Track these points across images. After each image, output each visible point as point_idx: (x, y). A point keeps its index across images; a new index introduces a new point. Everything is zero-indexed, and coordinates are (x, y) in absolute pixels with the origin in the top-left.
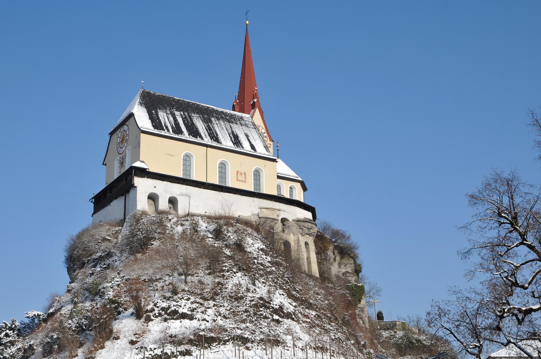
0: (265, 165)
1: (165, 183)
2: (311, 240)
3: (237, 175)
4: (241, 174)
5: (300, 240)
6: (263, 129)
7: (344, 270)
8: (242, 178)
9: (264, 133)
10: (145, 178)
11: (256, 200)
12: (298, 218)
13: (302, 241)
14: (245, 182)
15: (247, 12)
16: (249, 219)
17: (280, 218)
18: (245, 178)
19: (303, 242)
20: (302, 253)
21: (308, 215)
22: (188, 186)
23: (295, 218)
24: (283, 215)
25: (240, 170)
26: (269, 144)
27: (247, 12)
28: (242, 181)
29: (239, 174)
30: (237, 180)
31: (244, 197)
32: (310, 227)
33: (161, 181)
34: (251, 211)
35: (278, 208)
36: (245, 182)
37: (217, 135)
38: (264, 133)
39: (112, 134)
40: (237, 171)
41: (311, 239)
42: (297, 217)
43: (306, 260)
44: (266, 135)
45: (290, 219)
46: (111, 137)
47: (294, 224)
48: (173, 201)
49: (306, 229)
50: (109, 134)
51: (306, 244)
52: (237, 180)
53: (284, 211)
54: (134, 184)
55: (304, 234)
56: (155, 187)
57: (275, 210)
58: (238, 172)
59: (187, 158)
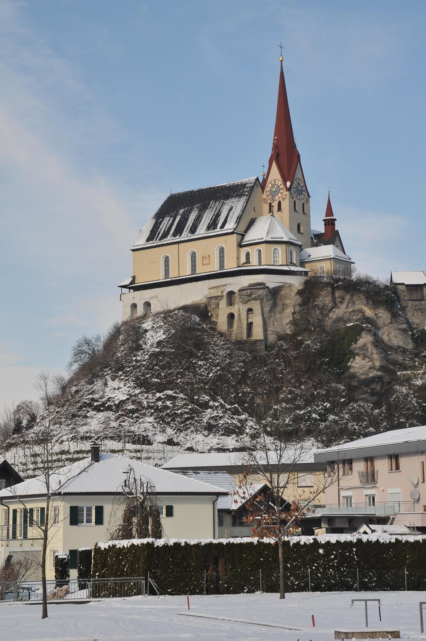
7: (350, 309)
9: (281, 185)
11: (207, 282)
16: (200, 302)
17: (225, 293)
23: (239, 288)
24: (228, 289)
28: (207, 264)
29: (204, 258)
30: (203, 265)
37: (200, 223)
38: (281, 185)
42: (242, 286)
48: (148, 305)
49: (245, 296)
52: (203, 265)
53: (229, 284)
55: (244, 302)
56: (134, 298)
58: (203, 256)
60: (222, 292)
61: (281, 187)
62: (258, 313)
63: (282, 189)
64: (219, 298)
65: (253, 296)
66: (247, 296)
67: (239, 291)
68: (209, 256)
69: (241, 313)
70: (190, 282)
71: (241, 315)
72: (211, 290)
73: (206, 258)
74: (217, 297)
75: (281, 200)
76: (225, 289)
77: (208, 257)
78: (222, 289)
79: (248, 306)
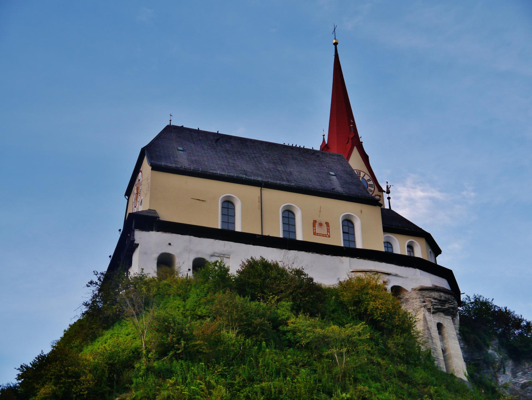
0: (361, 211)
1: (186, 238)
2: (449, 321)
3: (314, 226)
4: (321, 225)
5: (428, 319)
6: (366, 175)
9: (369, 180)
10: (152, 231)
11: (346, 260)
12: (421, 286)
13: (431, 321)
14: (327, 236)
15: (335, 29)
17: (389, 287)
18: (328, 231)
19: (433, 323)
20: (432, 339)
21: (443, 283)
22: (226, 242)
23: (417, 285)
24: (394, 282)
25: (319, 220)
26: (377, 195)
27: (335, 29)
28: (323, 235)
30: (315, 234)
31: (325, 256)
32: (443, 298)
33: (179, 235)
34: (337, 278)
36: (327, 236)
39: (128, 193)
40: (314, 221)
41: (450, 319)
43: (440, 352)
44: (371, 183)
45: (409, 289)
46: (128, 200)
47: (414, 295)
50: (125, 196)
51: (440, 326)
52: (315, 234)
54: (134, 241)
57: (380, 274)
58: (315, 222)
61: (369, 183)
62: (453, 336)
63: (371, 186)
65: (447, 306)
66: (439, 300)
68: (327, 224)
69: (429, 326)
70: (306, 251)
71: (430, 329)
77: (325, 225)
78: (386, 278)
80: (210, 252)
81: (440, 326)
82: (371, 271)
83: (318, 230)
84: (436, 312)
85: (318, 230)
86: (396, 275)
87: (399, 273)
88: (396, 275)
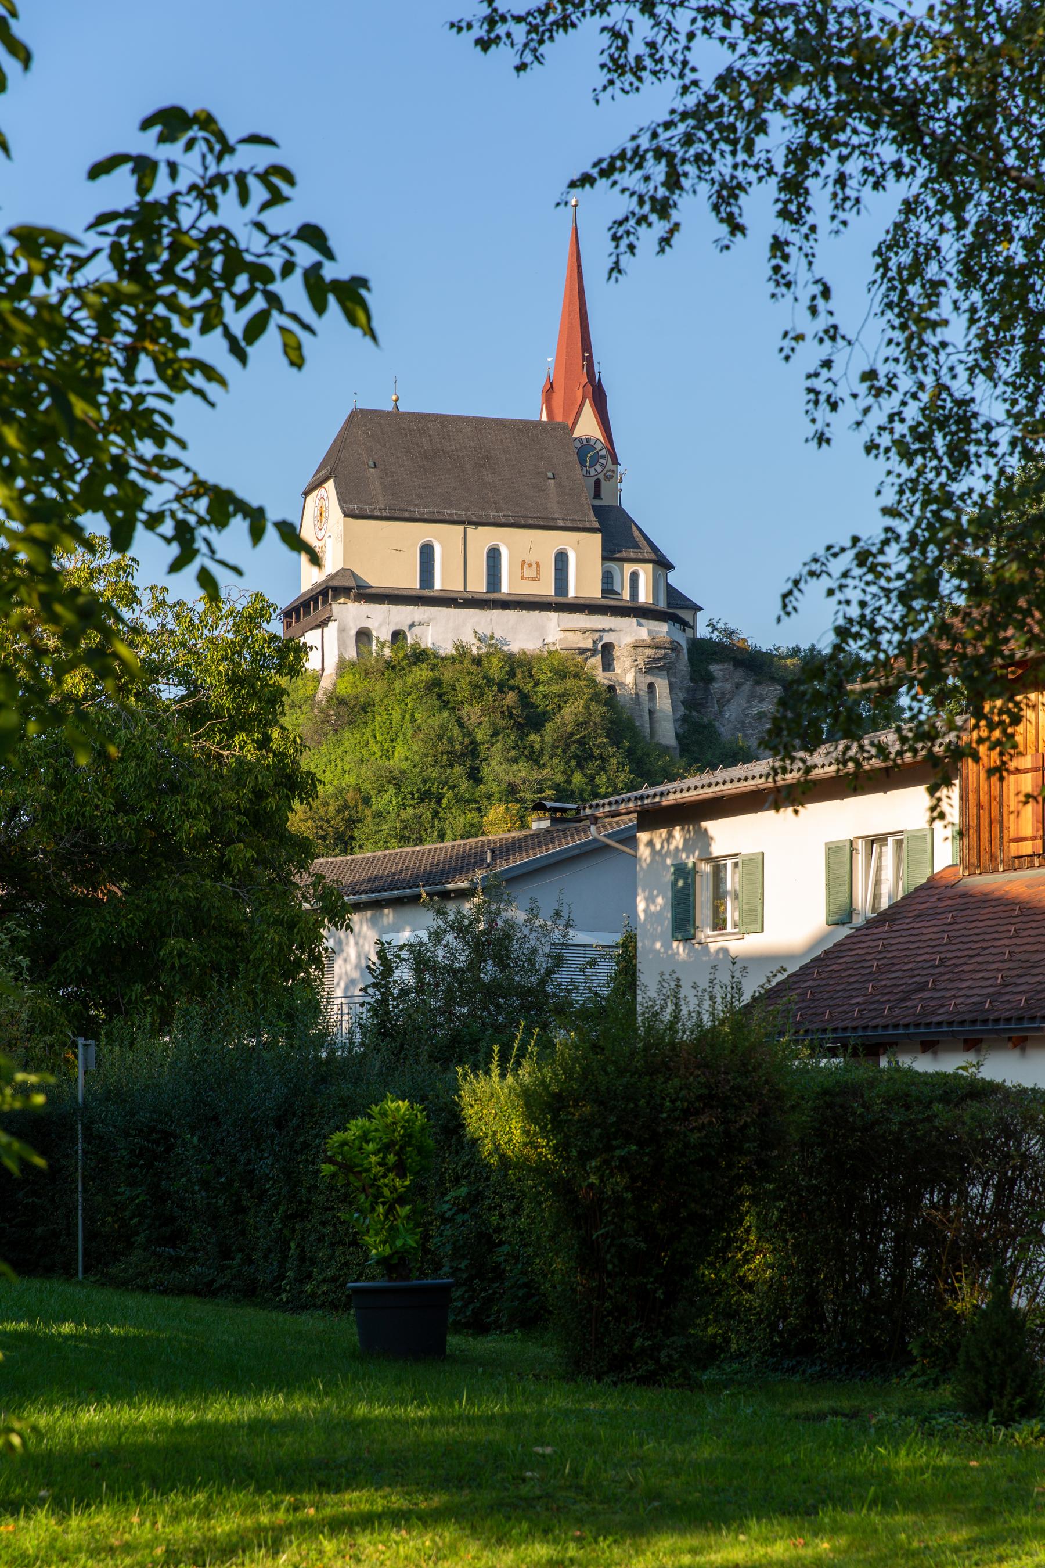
3: (522, 568)
4: (530, 565)
8: (529, 573)
11: (553, 616)
28: (532, 579)
30: (523, 578)
35: (600, 627)
52: (523, 578)
59: (427, 552)
60: (594, 642)
64: (589, 653)
67: (635, 647)
68: (537, 563)
72: (568, 634)
73: (530, 565)
74: (583, 651)
75: (601, 477)
76: (601, 638)
78: (597, 635)
79: (649, 679)
80: (409, 622)
81: (651, 686)
82: (580, 630)
83: (528, 573)
84: (649, 671)
85: (528, 573)
86: (611, 630)
87: (612, 626)
88: (611, 630)
